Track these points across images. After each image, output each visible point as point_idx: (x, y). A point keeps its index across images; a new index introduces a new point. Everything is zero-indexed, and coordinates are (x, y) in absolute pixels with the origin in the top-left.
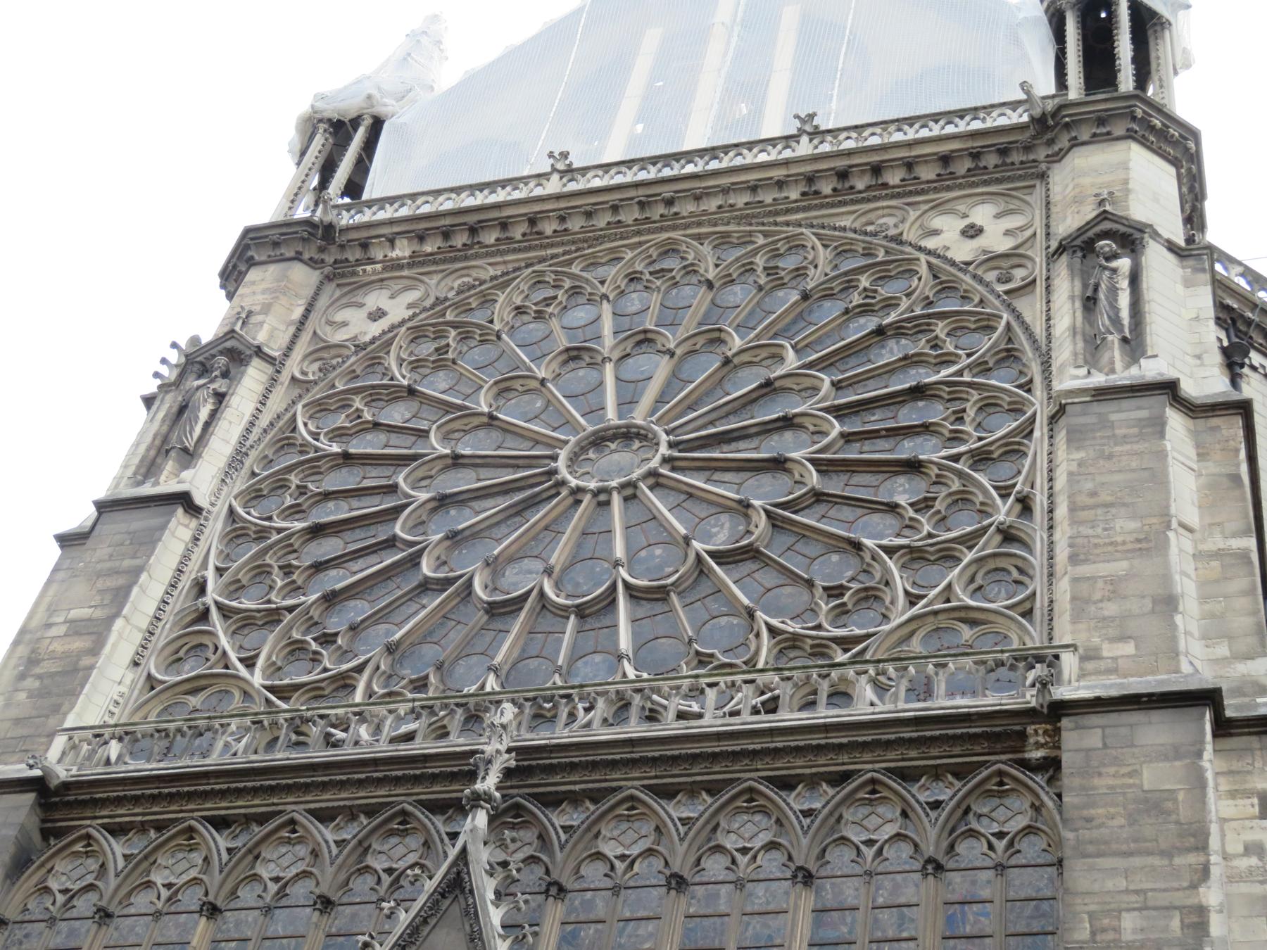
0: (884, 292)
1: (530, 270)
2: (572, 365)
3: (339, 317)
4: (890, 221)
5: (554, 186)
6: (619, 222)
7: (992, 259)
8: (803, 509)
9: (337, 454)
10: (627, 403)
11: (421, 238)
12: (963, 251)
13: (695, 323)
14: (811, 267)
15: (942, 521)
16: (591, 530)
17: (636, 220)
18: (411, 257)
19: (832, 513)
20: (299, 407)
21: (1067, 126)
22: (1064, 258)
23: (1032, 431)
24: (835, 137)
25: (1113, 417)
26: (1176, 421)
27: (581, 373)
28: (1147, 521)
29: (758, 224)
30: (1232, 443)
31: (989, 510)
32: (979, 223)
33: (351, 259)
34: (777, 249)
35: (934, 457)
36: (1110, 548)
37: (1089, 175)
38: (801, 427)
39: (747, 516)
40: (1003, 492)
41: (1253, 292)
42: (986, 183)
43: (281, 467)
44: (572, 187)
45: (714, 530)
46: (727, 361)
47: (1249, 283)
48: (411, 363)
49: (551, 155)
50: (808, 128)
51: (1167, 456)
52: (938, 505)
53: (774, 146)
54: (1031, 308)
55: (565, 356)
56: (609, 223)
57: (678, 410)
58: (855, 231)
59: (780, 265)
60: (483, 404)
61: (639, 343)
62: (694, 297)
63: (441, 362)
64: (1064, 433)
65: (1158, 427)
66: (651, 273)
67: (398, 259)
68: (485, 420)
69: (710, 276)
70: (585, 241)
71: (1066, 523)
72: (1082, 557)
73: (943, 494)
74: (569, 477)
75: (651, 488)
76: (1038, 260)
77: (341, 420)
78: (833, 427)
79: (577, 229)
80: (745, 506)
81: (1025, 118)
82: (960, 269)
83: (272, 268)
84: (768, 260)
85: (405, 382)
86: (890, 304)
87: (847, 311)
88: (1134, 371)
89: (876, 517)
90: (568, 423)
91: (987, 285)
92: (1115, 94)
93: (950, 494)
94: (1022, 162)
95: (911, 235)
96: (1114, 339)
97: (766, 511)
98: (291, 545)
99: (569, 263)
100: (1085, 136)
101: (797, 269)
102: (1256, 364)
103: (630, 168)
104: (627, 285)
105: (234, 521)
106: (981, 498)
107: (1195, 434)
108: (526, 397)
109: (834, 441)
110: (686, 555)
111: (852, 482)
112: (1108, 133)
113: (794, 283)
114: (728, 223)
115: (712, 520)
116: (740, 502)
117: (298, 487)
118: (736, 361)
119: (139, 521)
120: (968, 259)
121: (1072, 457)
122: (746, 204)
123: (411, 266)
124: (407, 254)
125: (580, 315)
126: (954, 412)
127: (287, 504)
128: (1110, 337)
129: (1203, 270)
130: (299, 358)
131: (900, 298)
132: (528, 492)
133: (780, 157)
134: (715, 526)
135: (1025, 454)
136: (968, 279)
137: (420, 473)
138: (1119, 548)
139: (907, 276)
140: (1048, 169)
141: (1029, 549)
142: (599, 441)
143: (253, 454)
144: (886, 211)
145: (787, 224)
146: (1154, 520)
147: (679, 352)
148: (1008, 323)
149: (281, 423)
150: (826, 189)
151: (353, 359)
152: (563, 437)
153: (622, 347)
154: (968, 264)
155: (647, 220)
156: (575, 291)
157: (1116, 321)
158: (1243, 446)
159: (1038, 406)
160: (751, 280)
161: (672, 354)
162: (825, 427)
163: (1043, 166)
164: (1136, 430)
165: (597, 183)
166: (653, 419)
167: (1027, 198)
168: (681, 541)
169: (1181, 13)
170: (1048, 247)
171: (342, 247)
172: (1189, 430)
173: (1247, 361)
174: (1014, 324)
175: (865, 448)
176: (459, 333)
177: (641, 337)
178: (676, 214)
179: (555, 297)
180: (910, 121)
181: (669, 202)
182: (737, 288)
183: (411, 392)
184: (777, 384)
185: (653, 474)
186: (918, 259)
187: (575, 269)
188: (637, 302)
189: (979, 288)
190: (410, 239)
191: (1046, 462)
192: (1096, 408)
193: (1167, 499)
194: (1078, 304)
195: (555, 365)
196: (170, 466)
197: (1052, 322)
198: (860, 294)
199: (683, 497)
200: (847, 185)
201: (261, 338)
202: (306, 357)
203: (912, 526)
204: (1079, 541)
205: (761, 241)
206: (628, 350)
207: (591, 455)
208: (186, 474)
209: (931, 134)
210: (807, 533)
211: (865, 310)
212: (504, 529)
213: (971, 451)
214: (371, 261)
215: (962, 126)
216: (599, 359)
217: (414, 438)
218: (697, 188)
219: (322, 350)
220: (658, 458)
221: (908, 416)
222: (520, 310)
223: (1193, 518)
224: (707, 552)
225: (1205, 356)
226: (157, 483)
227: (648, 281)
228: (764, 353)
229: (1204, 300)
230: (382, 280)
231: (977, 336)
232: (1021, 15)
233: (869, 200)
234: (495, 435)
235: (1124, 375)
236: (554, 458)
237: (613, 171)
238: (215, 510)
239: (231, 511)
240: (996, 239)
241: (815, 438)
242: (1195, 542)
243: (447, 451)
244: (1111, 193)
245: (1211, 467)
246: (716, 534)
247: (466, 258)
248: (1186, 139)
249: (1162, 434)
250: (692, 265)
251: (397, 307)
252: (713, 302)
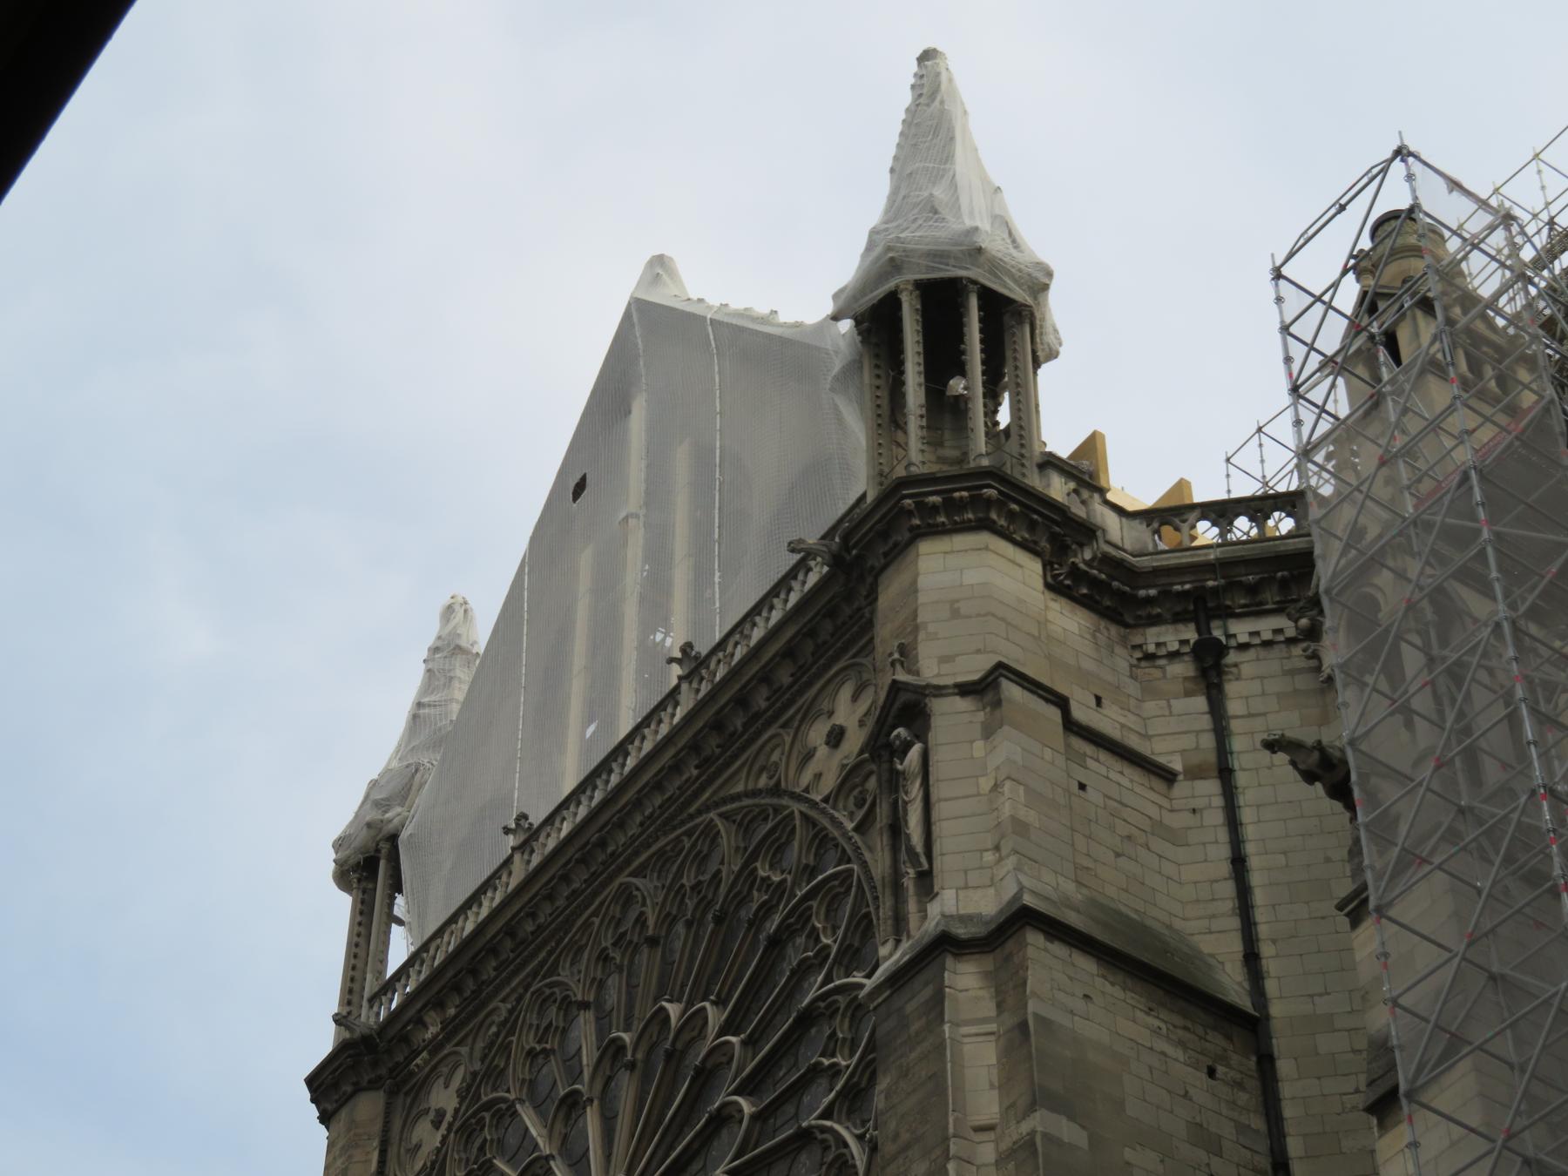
13: (650, 1001)
18: (442, 1029)
33: (401, 1058)
49: (507, 831)
67: (435, 1037)
114: (657, 839)
123: (448, 1039)
144: (769, 746)
164: (924, 1020)
184: (709, 1065)
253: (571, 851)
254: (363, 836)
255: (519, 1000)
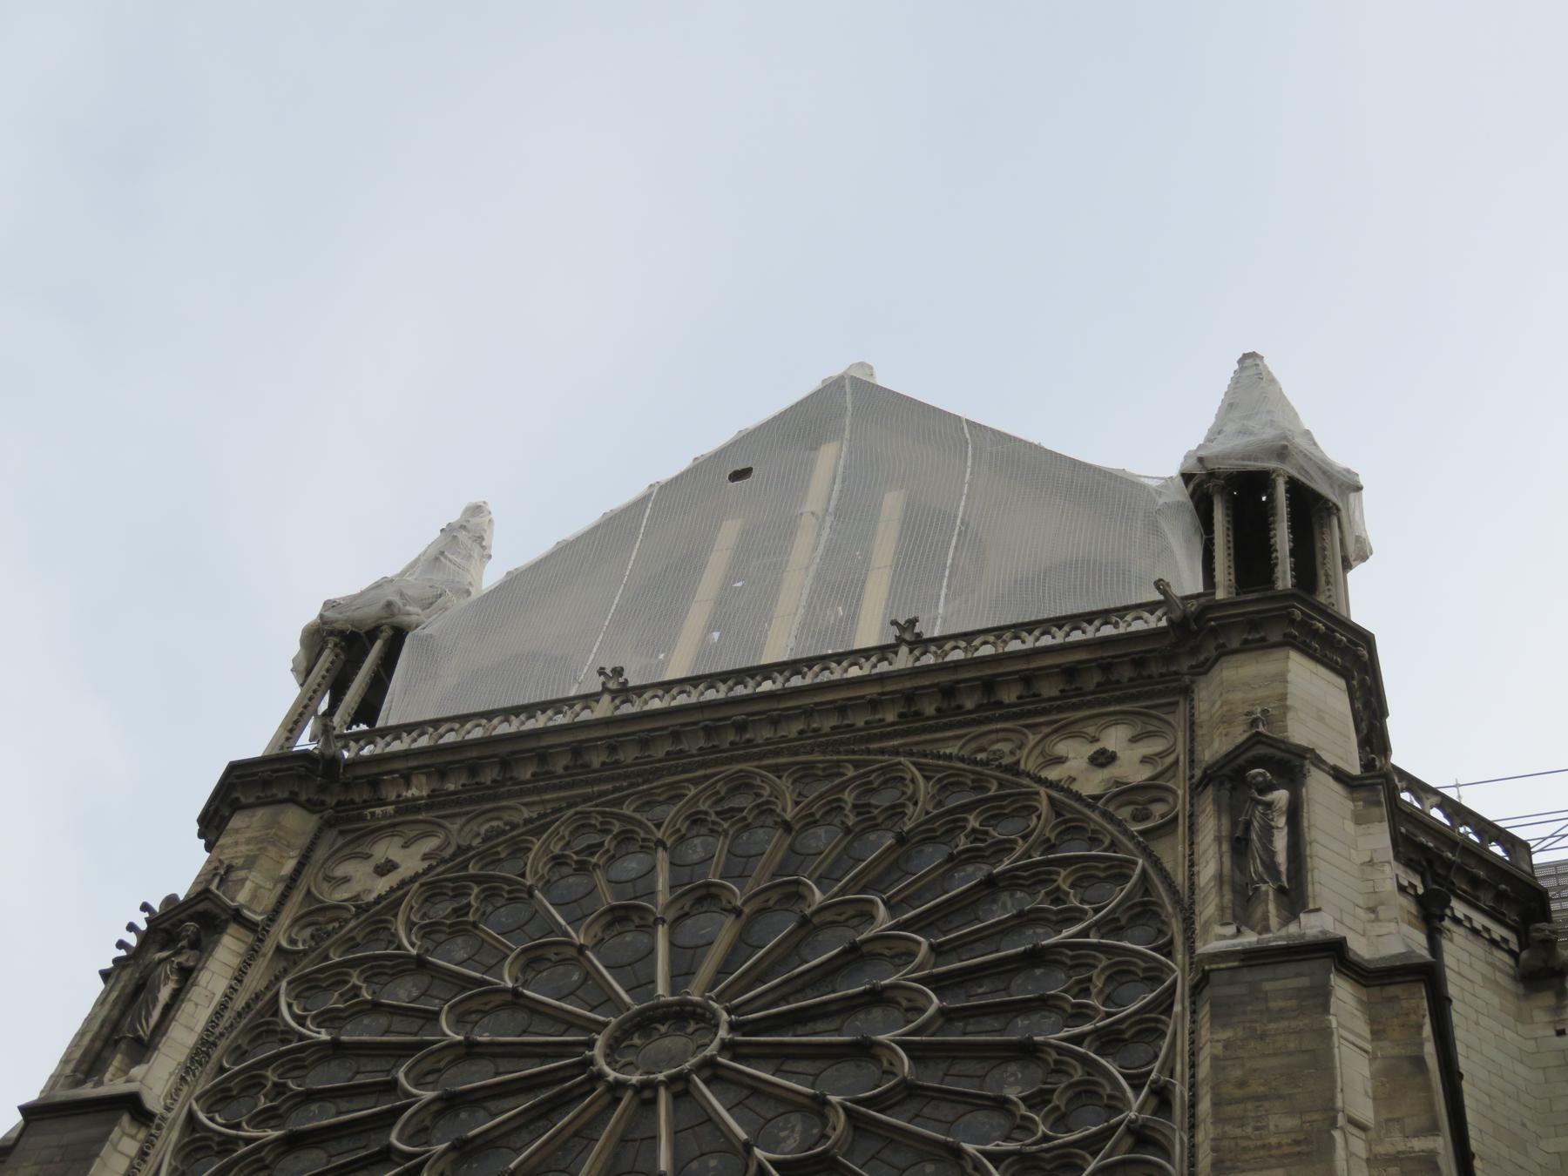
0: (995, 834)
1: (572, 811)
2: (618, 928)
3: (340, 871)
4: (1005, 747)
5: (603, 709)
6: (617, 762)
7: (1126, 793)
8: (891, 1107)
9: (324, 1043)
10: (680, 975)
11: (442, 773)
12: (1092, 783)
13: (768, 874)
14: (910, 805)
15: (1061, 1121)
16: (631, 1136)
17: (701, 749)
18: (429, 797)
19: (927, 1111)
20: (284, 984)
21: (1213, 632)
22: (1210, 792)
23: (1171, 1005)
24: (940, 647)
25: (1267, 986)
26: (1343, 992)
27: (628, 937)
28: (1307, 1118)
29: (847, 752)
30: (1413, 1017)
31: (1120, 1105)
32: (1111, 749)
33: (357, 799)
34: (870, 783)
35: (1052, 1038)
36: (1262, 1153)
37: (1233, 688)
38: (892, 1002)
39: (824, 1119)
40: (1136, 1082)
41: (1454, 827)
42: (1119, 700)
43: (251, 1058)
44: (627, 709)
45: (783, 1134)
46: (804, 921)
47: (1446, 816)
48: (422, 927)
49: (601, 672)
50: (908, 637)
51: (1331, 1034)
52: (1056, 1100)
53: (868, 659)
54: (1171, 854)
55: (609, 918)
56: (668, 753)
57: (743, 983)
58: (962, 760)
59: (873, 801)
60: (506, 977)
61: (699, 901)
62: (768, 842)
63: (460, 927)
64: (1207, 1008)
65: (1321, 998)
66: (718, 814)
67: (414, 799)
68: (509, 997)
69: (788, 816)
70: (639, 775)
71: (1209, 1120)
72: (1228, 1164)
73: (1062, 1086)
74: (607, 1069)
75: (707, 1082)
76: (1180, 792)
77: (334, 1001)
78: (931, 1002)
79: (629, 761)
80: (818, 1106)
81: (1164, 623)
82: (1088, 805)
83: (261, 814)
84: (857, 797)
85: (414, 952)
86: (1004, 848)
87: (951, 858)
88: (1293, 929)
89: (981, 1116)
90: (609, 1001)
91: (1119, 823)
92: (1269, 593)
93: (1071, 1086)
94: (1162, 675)
95: (1029, 765)
96: (1268, 888)
97: (845, 1109)
98: (262, 1160)
99: (619, 802)
100: (1235, 644)
101: (893, 807)
102: (1459, 915)
103: (696, 687)
104: (689, 829)
105: (194, 1131)
106: (1108, 1090)
107: (1367, 1006)
108: (561, 969)
109: (932, 1019)
110: (747, 1168)
111: (952, 1071)
112: (1263, 639)
113: (889, 824)
114: (812, 752)
115: (780, 1122)
116: (814, 1097)
117: (275, 1085)
118: (816, 920)
119: (73, 1132)
120: (1097, 792)
121: (1216, 1037)
122: (833, 728)
123: (429, 807)
124: (425, 793)
125: (631, 865)
126: (1078, 982)
127: (260, 1108)
128: (1264, 887)
129: (1379, 804)
130: (288, 922)
131: (1015, 841)
132: (556, 1089)
133: (875, 671)
134: (784, 1129)
135: (1163, 1034)
136: (1095, 816)
137: (425, 1066)
138: (1274, 1152)
139: (1025, 813)
140: (1193, 682)
141: (1168, 1155)
142: (645, 1022)
143: (223, 1044)
144: (1000, 735)
145: (882, 751)
146: (1316, 1116)
147: (747, 910)
148: (1144, 871)
149: (260, 1004)
150: (930, 709)
151: (352, 924)
152: (602, 1018)
153: (679, 905)
154: (1097, 798)
155: (715, 749)
156: (625, 838)
157: (1271, 867)
158: (1427, 1020)
159: (1178, 973)
160: (837, 821)
161: (738, 912)
162: (921, 1002)
163: (1187, 679)
164: (1293, 1003)
165: (656, 704)
166: (712, 994)
167: (1169, 718)
168: (740, 1148)
169: (1352, 496)
170: (1192, 777)
171: (347, 786)
172: (1360, 1002)
173: (1448, 912)
174: (1151, 871)
175: (970, 1028)
176: (484, 890)
177: (703, 892)
178: (749, 741)
179: (601, 844)
180: (1029, 627)
181: (741, 727)
182: (821, 831)
183: (420, 964)
184: (865, 949)
185: (710, 1063)
186: (1037, 793)
187: (627, 810)
188: (699, 849)
189: (1109, 827)
190: (428, 775)
191: (1187, 1043)
192: (1247, 975)
193: (1333, 1088)
194: (1225, 847)
195: (597, 929)
196: (117, 1061)
197: (1196, 869)
198: (967, 837)
199: (746, 1092)
200: (953, 704)
201: (242, 897)
202: (295, 921)
203: (1026, 1126)
204: (1225, 1143)
205: (851, 772)
206: (687, 909)
207: (636, 1041)
208: (137, 1071)
209: (1024, 647)
210: (896, 1137)
211: (973, 856)
212: (525, 1136)
213: (1096, 1030)
214: (382, 802)
215: (1091, 632)
216: (651, 919)
217: (420, 1022)
218: (775, 709)
219: (317, 915)
220: (717, 1042)
221: (1023, 988)
222: (558, 861)
223: (1365, 1111)
224: (773, 1163)
225: (1381, 909)
226: (100, 1083)
227: (714, 823)
228: (850, 911)
229: (1380, 838)
230: (394, 825)
231: (1108, 886)
232: (1161, 501)
233: (978, 722)
234: (522, 1017)
235: (1279, 934)
236: (590, 1045)
237: (674, 691)
238: (171, 1115)
239: (191, 1116)
240: (1132, 767)
241: (909, 1015)
242: (1369, 1143)
243: (460, 1038)
244: (1265, 712)
245: (1389, 1048)
246: (784, 1140)
247: (496, 798)
248: (1357, 645)
249: (1326, 1008)
250: (768, 802)
251: (410, 861)
252: (791, 848)
253: (708, 715)
254: (371, 612)
255: (559, 810)
